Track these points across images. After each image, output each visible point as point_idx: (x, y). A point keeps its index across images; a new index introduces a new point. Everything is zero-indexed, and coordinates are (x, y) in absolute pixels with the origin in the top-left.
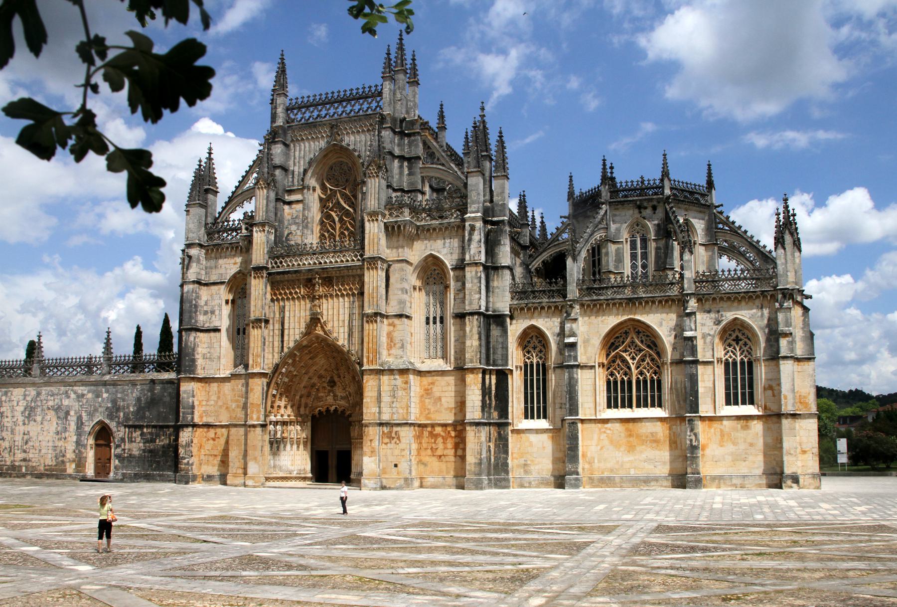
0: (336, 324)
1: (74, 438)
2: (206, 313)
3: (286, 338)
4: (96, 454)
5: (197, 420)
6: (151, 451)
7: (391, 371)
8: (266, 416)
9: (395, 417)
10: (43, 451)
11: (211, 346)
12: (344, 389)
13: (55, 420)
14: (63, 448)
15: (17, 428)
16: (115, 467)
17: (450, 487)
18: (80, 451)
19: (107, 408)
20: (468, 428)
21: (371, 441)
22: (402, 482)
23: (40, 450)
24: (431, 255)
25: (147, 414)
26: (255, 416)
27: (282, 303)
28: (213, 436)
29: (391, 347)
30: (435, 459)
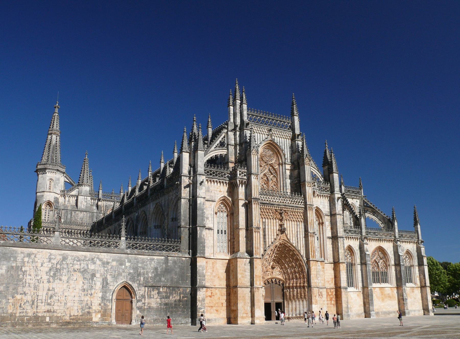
1: (100, 295)
4: (117, 307)
6: (166, 304)
9: (320, 285)
10: (69, 304)
13: (81, 280)
14: (89, 302)
15: (41, 285)
16: (137, 316)
18: (105, 304)
19: (130, 273)
20: (342, 290)
23: (66, 304)
25: (163, 279)
26: (258, 283)
28: (210, 294)
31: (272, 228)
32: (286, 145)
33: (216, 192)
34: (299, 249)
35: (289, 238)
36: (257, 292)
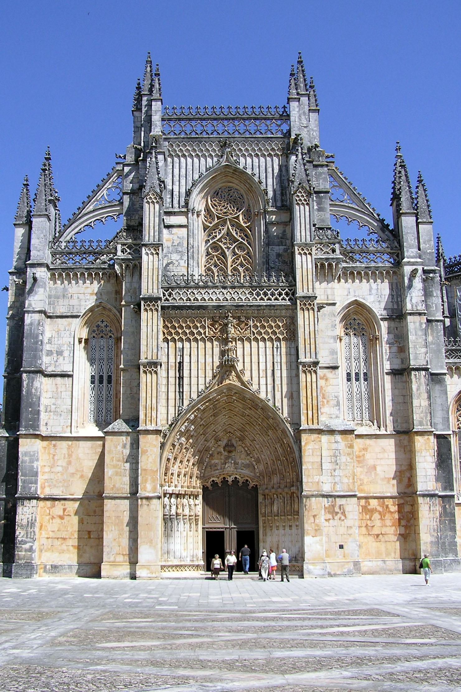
2: (50, 353)
3: (186, 388)
5: (39, 493)
7: (332, 432)
8: (162, 486)
9: (338, 487)
11: (56, 395)
12: (248, 455)
17: (391, 572)
20: (420, 500)
22: (351, 566)
24: (356, 303)
26: (149, 486)
27: (179, 345)
28: (61, 513)
29: (323, 405)
30: (371, 538)
31: (202, 360)
32: (270, 170)
33: (81, 296)
34: (278, 404)
35: (246, 378)
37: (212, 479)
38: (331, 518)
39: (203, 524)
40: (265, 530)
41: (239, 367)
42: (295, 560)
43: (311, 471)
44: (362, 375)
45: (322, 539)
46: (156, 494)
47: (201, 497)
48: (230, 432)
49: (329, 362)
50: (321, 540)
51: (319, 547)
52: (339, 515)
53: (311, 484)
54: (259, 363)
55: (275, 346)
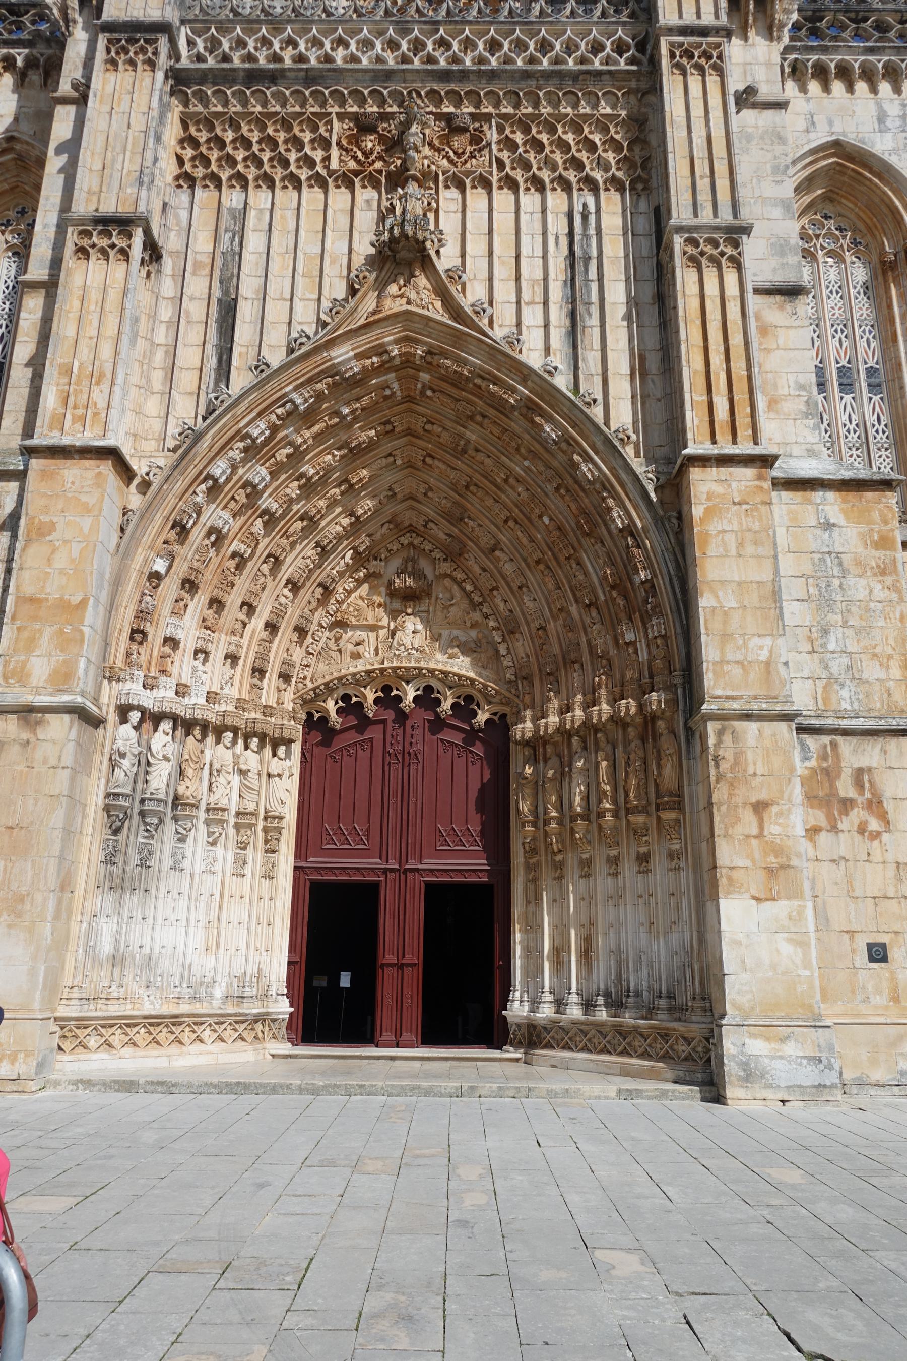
0: (504, 292)
3: (244, 333)
9: (845, 698)
21: (760, 808)
24: (837, 147)
26: (40, 668)
31: (309, 245)
36: (14, 751)
37: (341, 692)
38: (823, 822)
39: (301, 851)
40: (535, 880)
41: (446, 260)
42: (670, 1010)
43: (735, 617)
44: (863, 375)
45: (801, 911)
46: (65, 698)
47: (296, 748)
48: (411, 529)
49: (770, 278)
50: (797, 918)
51: (787, 949)
52: (857, 815)
53: (737, 671)
54: (518, 257)
55: (578, 208)
